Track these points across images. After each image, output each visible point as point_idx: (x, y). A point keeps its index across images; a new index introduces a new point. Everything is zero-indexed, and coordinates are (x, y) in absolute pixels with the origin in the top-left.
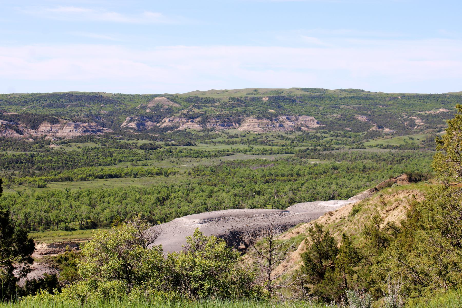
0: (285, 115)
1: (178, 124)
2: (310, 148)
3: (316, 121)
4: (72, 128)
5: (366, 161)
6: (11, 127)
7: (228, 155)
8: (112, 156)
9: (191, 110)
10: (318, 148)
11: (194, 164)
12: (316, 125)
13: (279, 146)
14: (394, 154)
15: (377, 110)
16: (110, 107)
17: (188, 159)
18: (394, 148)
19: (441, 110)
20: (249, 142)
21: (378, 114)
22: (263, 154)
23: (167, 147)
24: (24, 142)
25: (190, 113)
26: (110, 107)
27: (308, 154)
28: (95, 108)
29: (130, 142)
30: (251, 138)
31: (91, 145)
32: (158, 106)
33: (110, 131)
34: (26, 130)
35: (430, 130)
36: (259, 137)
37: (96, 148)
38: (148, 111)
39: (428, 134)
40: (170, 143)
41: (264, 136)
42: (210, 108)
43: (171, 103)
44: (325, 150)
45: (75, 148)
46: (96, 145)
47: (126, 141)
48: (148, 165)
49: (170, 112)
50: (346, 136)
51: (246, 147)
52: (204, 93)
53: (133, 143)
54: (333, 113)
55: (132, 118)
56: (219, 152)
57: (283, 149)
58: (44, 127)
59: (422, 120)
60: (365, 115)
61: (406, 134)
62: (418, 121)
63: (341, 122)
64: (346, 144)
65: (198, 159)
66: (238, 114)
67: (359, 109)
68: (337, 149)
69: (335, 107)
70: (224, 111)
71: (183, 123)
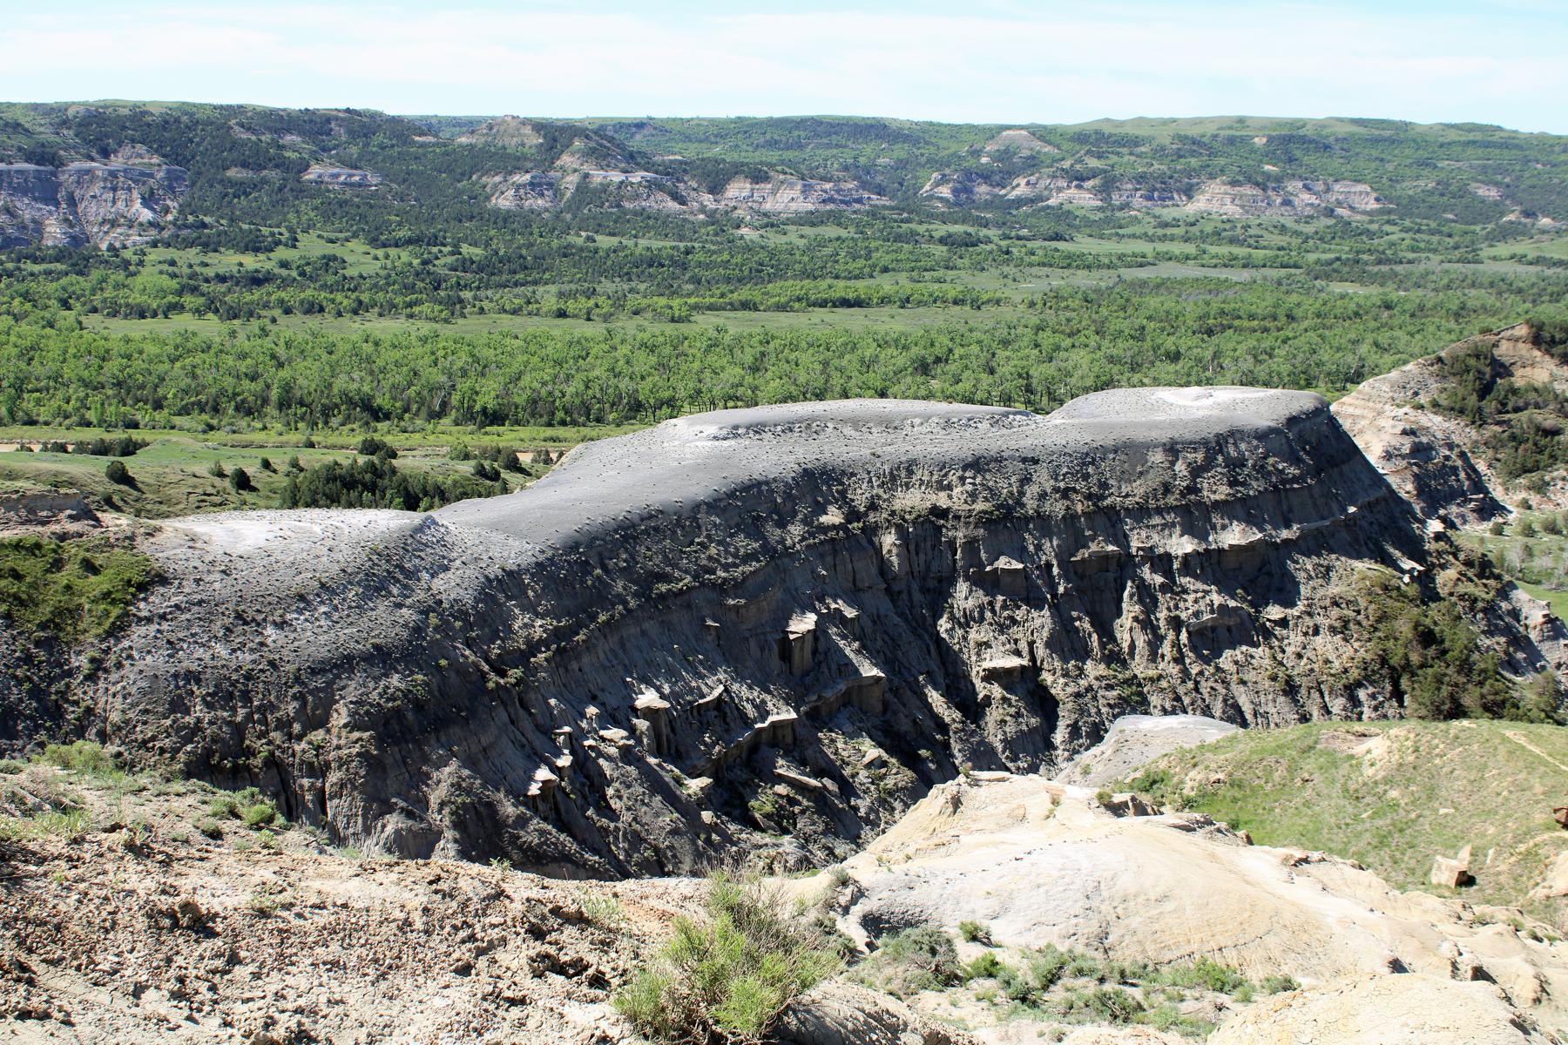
0: (1301, 178)
1: (1046, 193)
2: (1344, 257)
3: (1374, 195)
4: (796, 192)
5: (1473, 292)
6: (661, 188)
7: (1141, 265)
8: (868, 257)
9: (1080, 161)
10: (1365, 257)
11: (1054, 283)
13: (1272, 249)
14: (1549, 277)
15: (1527, 174)
16: (900, 151)
17: (1046, 270)
18: (1555, 264)
20: (1204, 237)
21: (1529, 182)
22: (1225, 266)
23: (1004, 243)
24: (685, 220)
25: (1078, 167)
26: (900, 151)
27: (1335, 271)
28: (867, 151)
29: (921, 229)
30: (1209, 229)
31: (831, 231)
32: (1006, 151)
33: (885, 201)
34: (694, 194)
36: (1227, 226)
37: (838, 239)
38: (984, 160)
40: (1013, 234)
41: (1239, 225)
42: (1126, 158)
43: (1038, 145)
44: (1379, 262)
45: (794, 237)
46: (843, 233)
47: (913, 226)
48: (945, 281)
49: (1032, 164)
50: (1440, 232)
51: (1190, 249)
52: (1122, 123)
53: (927, 230)
54: (1418, 178)
55: (944, 176)
56: (1121, 257)
57: (1277, 256)
58: (737, 190)
60: (1496, 184)
63: (1436, 198)
64: (1435, 251)
65: (1067, 272)
66: (1189, 173)
67: (1484, 170)
68: (1410, 262)
69: (1425, 163)
70: (1156, 166)
71: (1060, 190)
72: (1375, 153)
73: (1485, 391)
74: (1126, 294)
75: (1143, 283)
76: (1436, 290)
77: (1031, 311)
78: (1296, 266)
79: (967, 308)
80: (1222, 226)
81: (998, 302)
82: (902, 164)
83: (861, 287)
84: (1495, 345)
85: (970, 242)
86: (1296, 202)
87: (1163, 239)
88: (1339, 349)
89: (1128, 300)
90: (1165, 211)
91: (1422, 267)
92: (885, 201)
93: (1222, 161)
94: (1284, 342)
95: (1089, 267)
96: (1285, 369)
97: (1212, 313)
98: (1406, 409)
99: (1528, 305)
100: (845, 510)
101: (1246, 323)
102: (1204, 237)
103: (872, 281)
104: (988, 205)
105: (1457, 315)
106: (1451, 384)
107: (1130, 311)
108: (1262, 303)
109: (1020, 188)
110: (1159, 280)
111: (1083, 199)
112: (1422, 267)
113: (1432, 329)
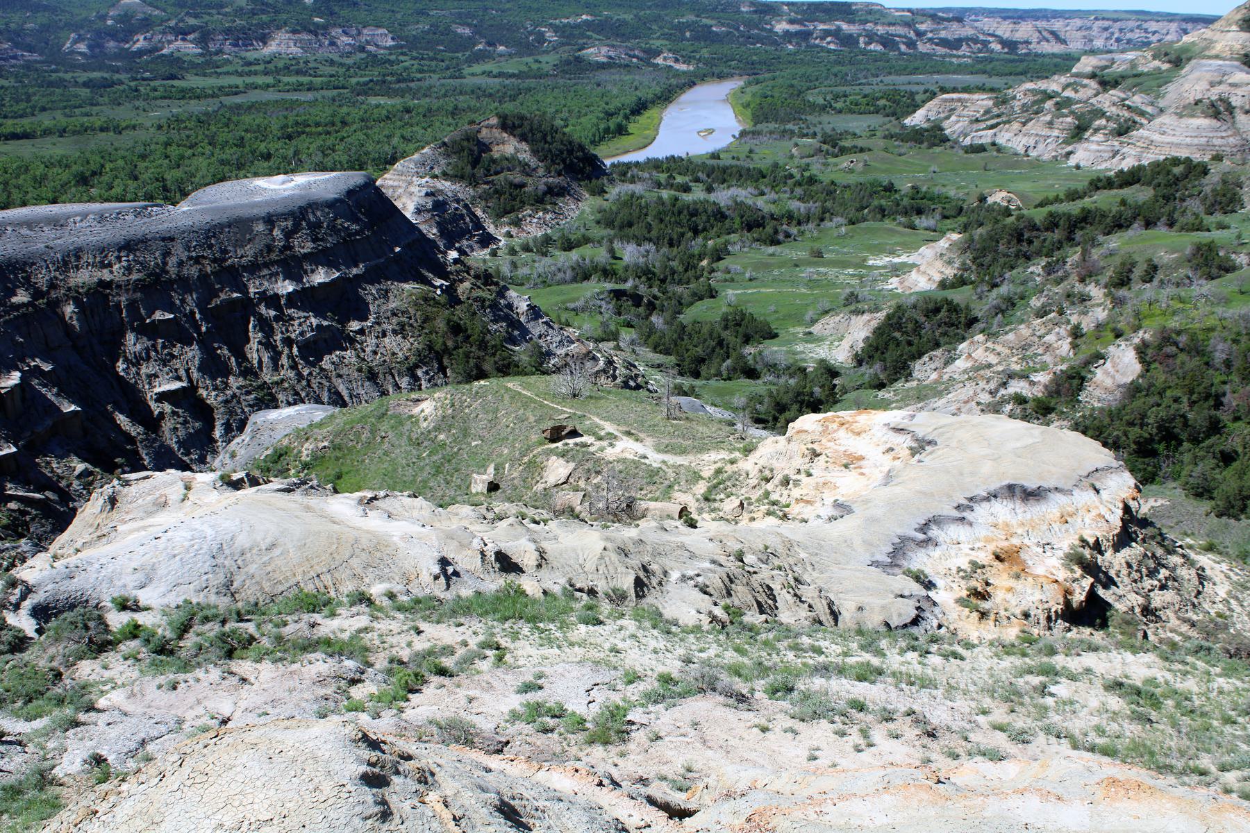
0: (340, 26)
5: (462, 98)
7: (236, 94)
8: (28, 101)
9: (182, 20)
10: (389, 78)
12: (390, 43)
19: (584, 17)
23: (133, 84)
25: (181, 25)
29: (68, 76)
30: (281, 65)
32: (126, 15)
33: (36, 57)
35: (567, 48)
36: (294, 62)
38: (109, 22)
39: (565, 53)
42: (216, 17)
44: (399, 81)
47: (61, 75)
49: (146, 24)
50: (436, 59)
51: (269, 80)
56: (221, 88)
59: (556, 32)
60: (469, 25)
61: (530, 55)
62: (550, 35)
63: (431, 36)
64: (434, 72)
65: (182, 102)
66: (262, 25)
67: (460, 15)
68: (419, 80)
71: (170, 42)
72: (388, 7)
73: (475, 162)
74: (228, 115)
75: (239, 107)
76: (437, 98)
78: (344, 88)
79: (111, 134)
80: (289, 62)
81: (134, 127)
82: (45, 28)
83: (26, 124)
84: (479, 131)
85: (107, 84)
86: (339, 43)
87: (249, 74)
88: (378, 142)
89: (229, 119)
90: (248, 54)
91: (427, 83)
92: (36, 57)
93: (284, 16)
94: (342, 140)
95: (198, 98)
96: (344, 158)
98: (427, 179)
99: (497, 104)
101: (314, 129)
102: (278, 71)
103: (33, 119)
104: (118, 56)
105: (453, 114)
106: (454, 160)
107: (232, 126)
108: (323, 114)
109: (140, 42)
111: (188, 48)
112: (427, 83)
113: (438, 124)
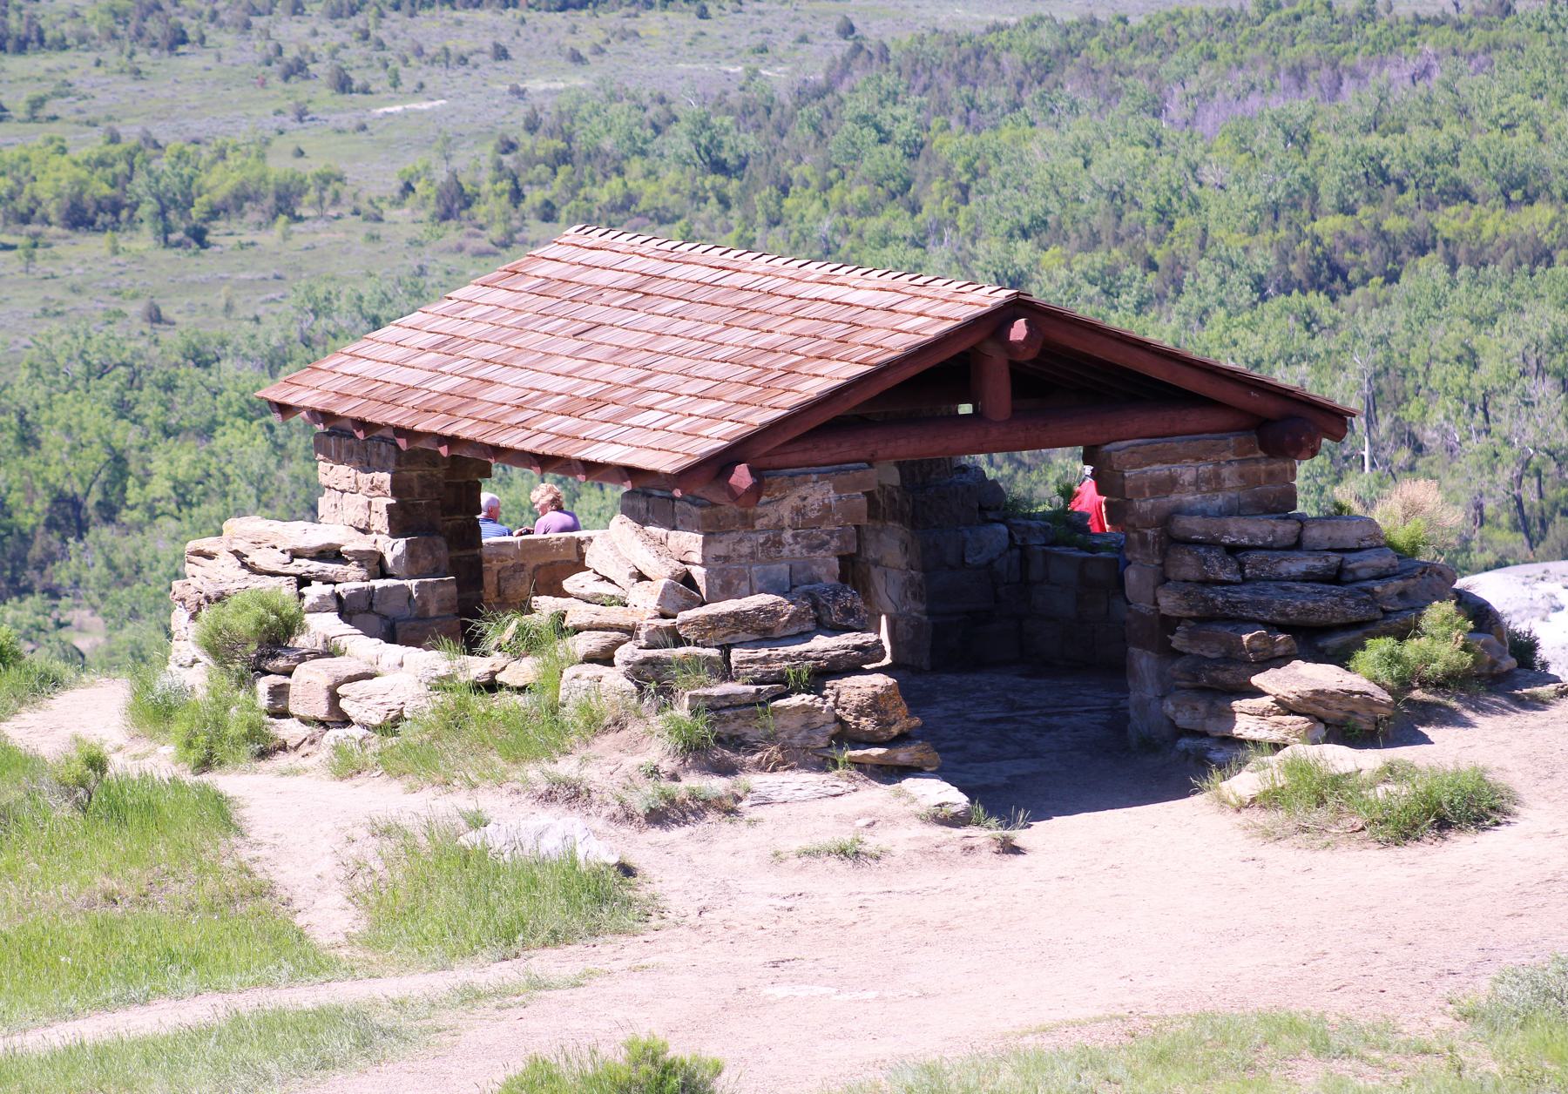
11: (536, 85)
74: (903, 119)
77: (452, 233)
79: (143, 241)
81: (285, 202)
89: (914, 150)
97: (1329, 184)
100: (191, 435)
101: (1494, 222)
107: (934, 200)
110: (1046, 38)
